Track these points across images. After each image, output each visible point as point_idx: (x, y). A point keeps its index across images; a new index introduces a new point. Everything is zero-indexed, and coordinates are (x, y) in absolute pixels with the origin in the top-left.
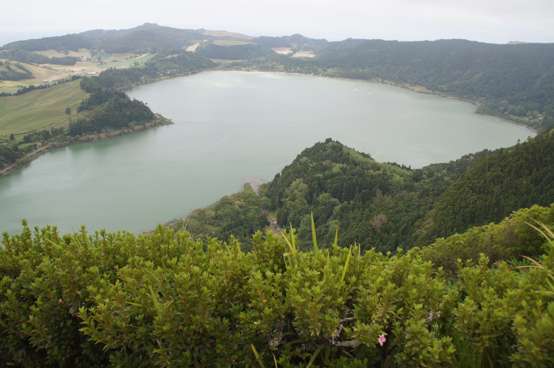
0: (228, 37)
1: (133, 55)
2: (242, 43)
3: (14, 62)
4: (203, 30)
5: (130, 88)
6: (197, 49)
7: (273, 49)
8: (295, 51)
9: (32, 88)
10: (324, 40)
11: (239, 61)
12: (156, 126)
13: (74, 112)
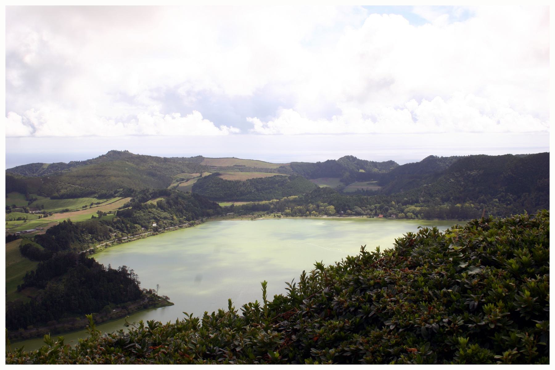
0: (239, 166)
1: (95, 200)
2: (263, 175)
4: (200, 158)
8: (347, 182)
10: (391, 163)
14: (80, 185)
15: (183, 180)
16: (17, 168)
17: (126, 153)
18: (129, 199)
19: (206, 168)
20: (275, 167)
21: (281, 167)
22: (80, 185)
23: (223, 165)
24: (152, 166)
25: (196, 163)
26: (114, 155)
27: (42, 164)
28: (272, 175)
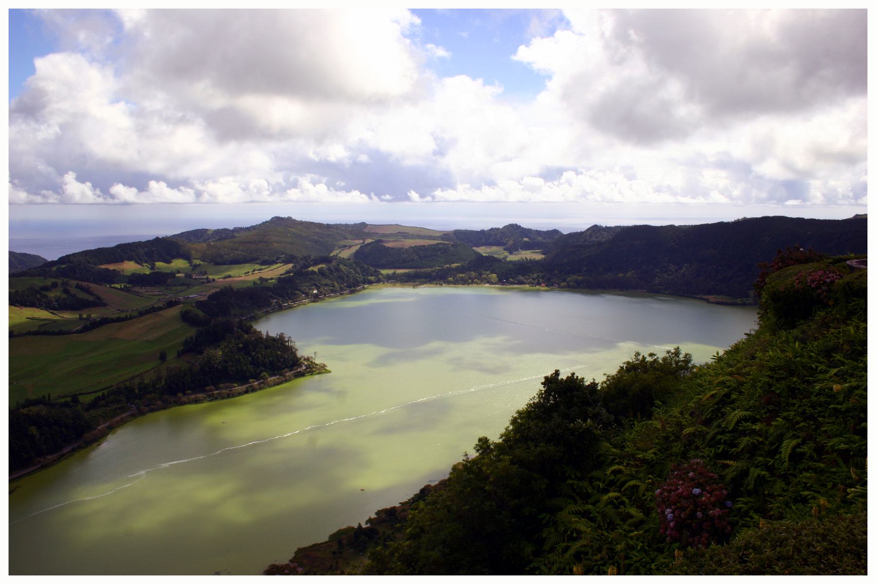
0: (403, 233)
1: (257, 267)
3: (74, 283)
4: (363, 225)
7: (474, 248)
9: (104, 322)
10: (555, 232)
11: (422, 270)
12: (302, 375)
13: (171, 356)
14: (242, 251)
15: (345, 246)
16: (182, 233)
17: (289, 219)
18: (290, 266)
19: (369, 235)
20: (438, 235)
22: (242, 251)
23: (387, 232)
24: (315, 233)
25: (359, 230)
26: (277, 221)
27: (207, 230)
28: (436, 242)
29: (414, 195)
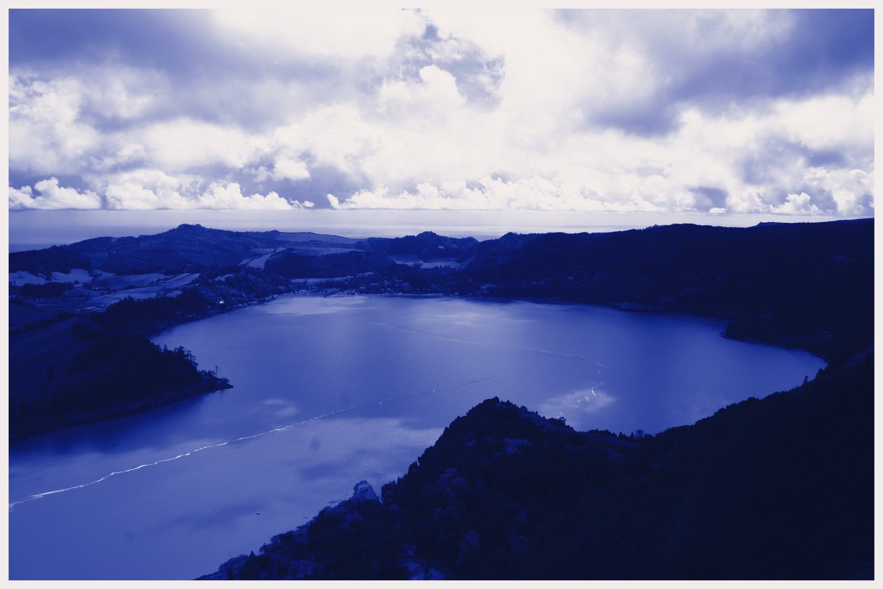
1: (162, 276)
4: (275, 233)
5: (158, 332)
6: (267, 263)
10: (470, 240)
17: (198, 226)
18: (197, 275)
19: (281, 243)
20: (352, 243)
21: (359, 243)
23: (299, 241)
25: (271, 238)
27: (110, 238)
28: (349, 250)
29: (333, 200)
